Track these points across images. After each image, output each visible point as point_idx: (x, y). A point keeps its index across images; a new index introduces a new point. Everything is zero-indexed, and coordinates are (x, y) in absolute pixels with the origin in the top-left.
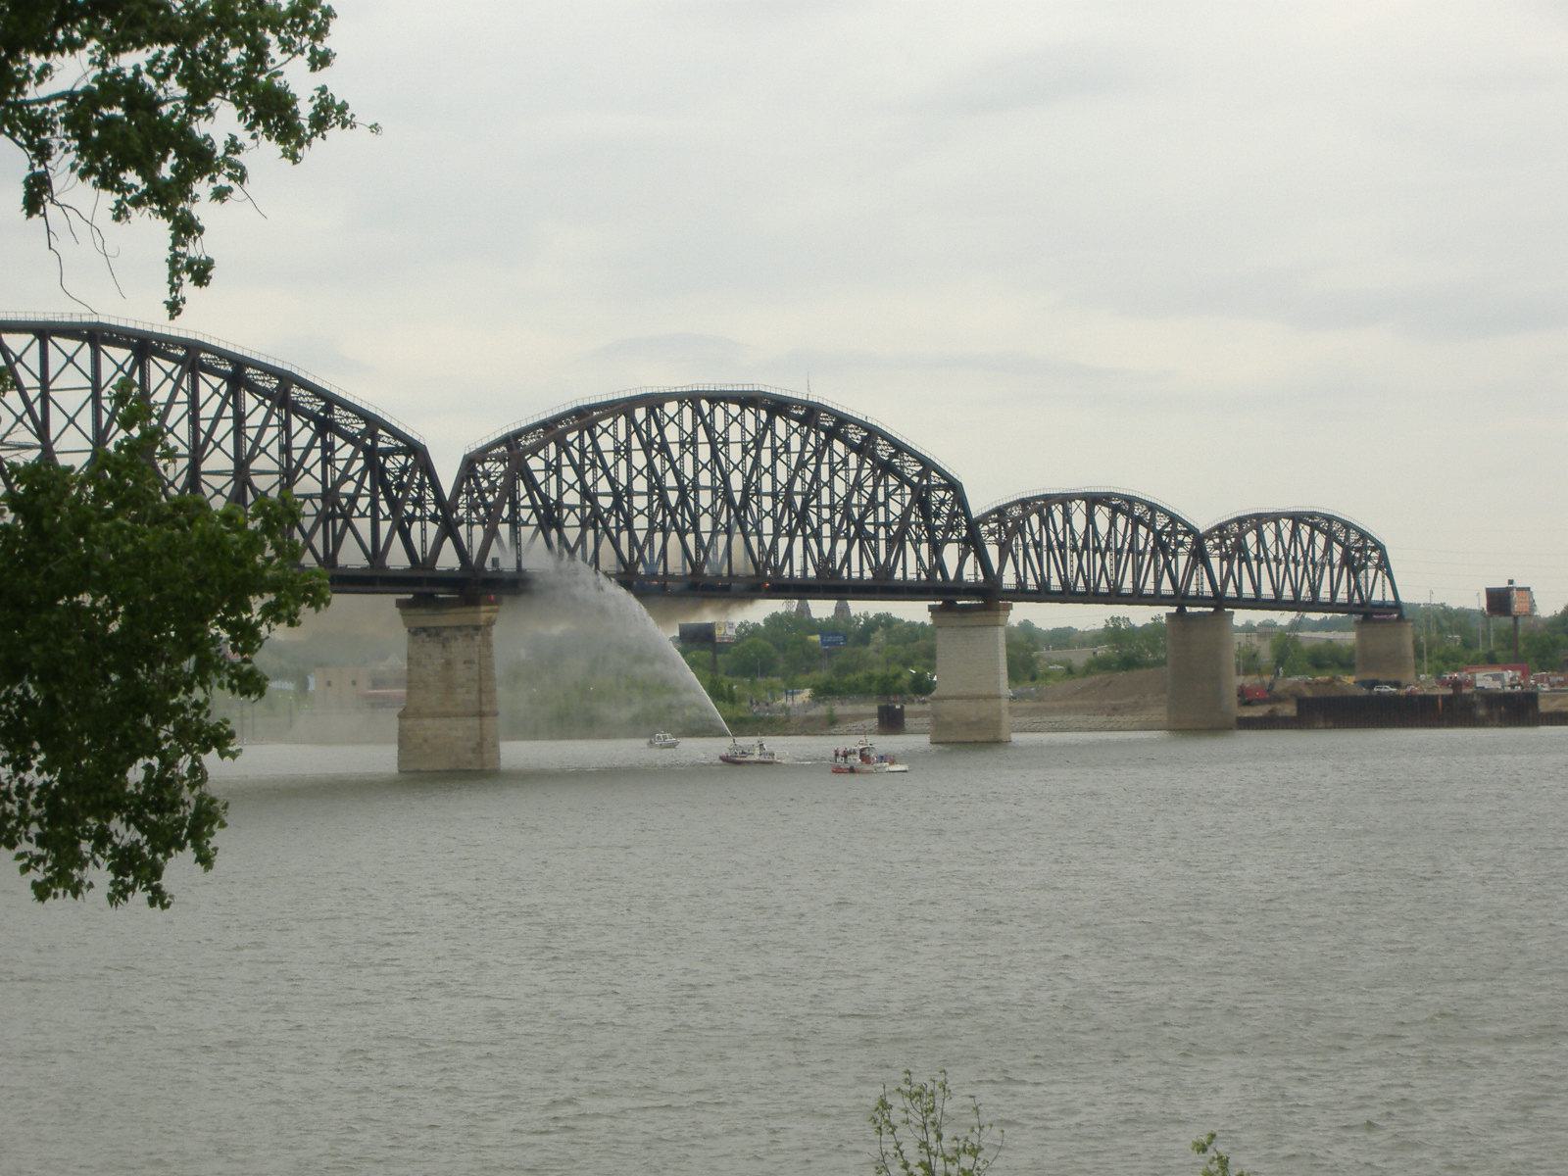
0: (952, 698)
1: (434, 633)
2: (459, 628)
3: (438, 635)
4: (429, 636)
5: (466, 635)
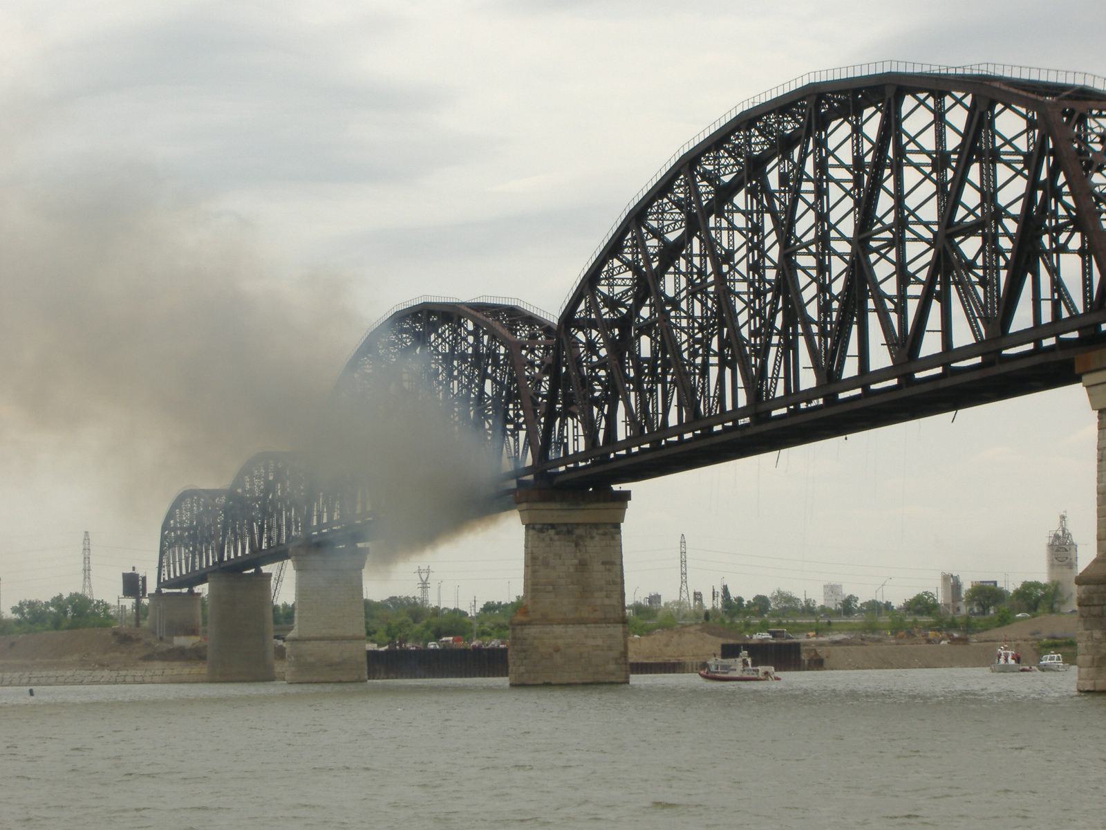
0: (316, 639)
1: (566, 530)
2: (596, 526)
3: (570, 532)
4: (557, 533)
5: (605, 534)
